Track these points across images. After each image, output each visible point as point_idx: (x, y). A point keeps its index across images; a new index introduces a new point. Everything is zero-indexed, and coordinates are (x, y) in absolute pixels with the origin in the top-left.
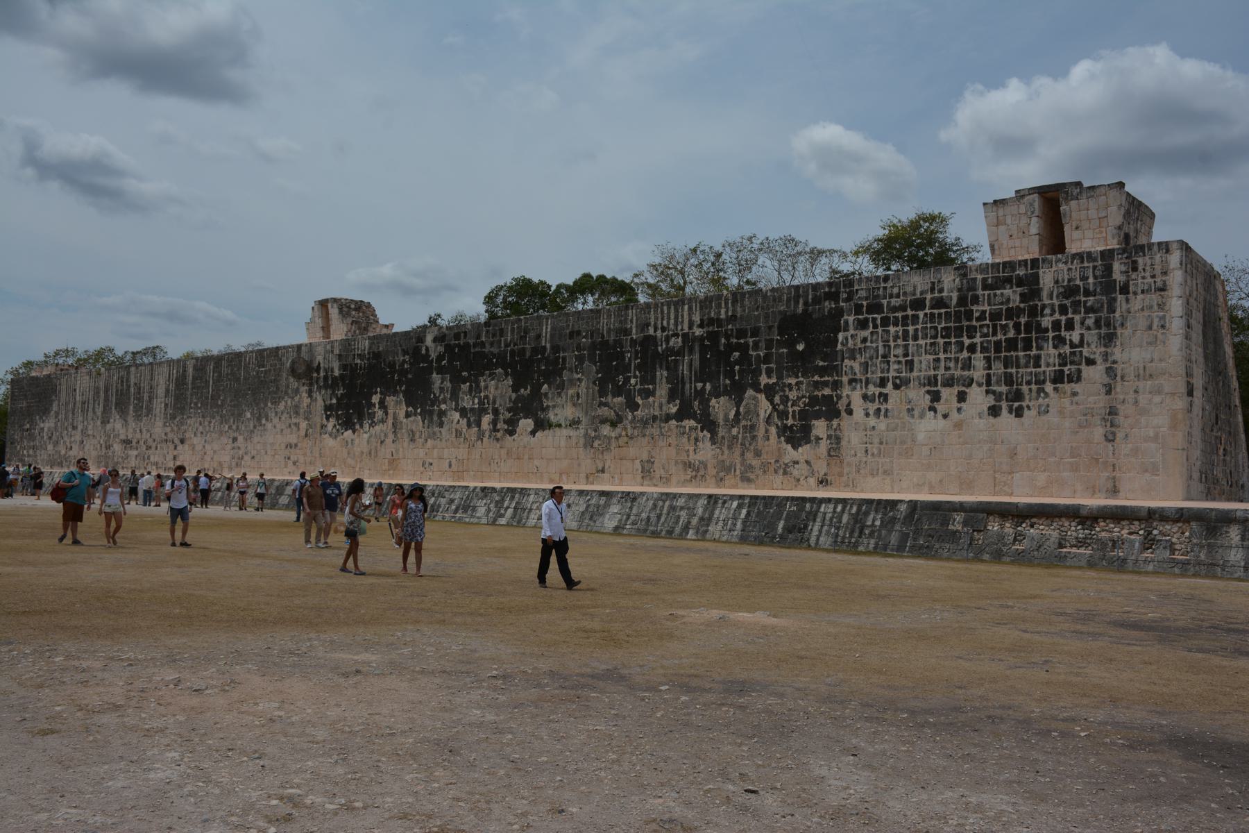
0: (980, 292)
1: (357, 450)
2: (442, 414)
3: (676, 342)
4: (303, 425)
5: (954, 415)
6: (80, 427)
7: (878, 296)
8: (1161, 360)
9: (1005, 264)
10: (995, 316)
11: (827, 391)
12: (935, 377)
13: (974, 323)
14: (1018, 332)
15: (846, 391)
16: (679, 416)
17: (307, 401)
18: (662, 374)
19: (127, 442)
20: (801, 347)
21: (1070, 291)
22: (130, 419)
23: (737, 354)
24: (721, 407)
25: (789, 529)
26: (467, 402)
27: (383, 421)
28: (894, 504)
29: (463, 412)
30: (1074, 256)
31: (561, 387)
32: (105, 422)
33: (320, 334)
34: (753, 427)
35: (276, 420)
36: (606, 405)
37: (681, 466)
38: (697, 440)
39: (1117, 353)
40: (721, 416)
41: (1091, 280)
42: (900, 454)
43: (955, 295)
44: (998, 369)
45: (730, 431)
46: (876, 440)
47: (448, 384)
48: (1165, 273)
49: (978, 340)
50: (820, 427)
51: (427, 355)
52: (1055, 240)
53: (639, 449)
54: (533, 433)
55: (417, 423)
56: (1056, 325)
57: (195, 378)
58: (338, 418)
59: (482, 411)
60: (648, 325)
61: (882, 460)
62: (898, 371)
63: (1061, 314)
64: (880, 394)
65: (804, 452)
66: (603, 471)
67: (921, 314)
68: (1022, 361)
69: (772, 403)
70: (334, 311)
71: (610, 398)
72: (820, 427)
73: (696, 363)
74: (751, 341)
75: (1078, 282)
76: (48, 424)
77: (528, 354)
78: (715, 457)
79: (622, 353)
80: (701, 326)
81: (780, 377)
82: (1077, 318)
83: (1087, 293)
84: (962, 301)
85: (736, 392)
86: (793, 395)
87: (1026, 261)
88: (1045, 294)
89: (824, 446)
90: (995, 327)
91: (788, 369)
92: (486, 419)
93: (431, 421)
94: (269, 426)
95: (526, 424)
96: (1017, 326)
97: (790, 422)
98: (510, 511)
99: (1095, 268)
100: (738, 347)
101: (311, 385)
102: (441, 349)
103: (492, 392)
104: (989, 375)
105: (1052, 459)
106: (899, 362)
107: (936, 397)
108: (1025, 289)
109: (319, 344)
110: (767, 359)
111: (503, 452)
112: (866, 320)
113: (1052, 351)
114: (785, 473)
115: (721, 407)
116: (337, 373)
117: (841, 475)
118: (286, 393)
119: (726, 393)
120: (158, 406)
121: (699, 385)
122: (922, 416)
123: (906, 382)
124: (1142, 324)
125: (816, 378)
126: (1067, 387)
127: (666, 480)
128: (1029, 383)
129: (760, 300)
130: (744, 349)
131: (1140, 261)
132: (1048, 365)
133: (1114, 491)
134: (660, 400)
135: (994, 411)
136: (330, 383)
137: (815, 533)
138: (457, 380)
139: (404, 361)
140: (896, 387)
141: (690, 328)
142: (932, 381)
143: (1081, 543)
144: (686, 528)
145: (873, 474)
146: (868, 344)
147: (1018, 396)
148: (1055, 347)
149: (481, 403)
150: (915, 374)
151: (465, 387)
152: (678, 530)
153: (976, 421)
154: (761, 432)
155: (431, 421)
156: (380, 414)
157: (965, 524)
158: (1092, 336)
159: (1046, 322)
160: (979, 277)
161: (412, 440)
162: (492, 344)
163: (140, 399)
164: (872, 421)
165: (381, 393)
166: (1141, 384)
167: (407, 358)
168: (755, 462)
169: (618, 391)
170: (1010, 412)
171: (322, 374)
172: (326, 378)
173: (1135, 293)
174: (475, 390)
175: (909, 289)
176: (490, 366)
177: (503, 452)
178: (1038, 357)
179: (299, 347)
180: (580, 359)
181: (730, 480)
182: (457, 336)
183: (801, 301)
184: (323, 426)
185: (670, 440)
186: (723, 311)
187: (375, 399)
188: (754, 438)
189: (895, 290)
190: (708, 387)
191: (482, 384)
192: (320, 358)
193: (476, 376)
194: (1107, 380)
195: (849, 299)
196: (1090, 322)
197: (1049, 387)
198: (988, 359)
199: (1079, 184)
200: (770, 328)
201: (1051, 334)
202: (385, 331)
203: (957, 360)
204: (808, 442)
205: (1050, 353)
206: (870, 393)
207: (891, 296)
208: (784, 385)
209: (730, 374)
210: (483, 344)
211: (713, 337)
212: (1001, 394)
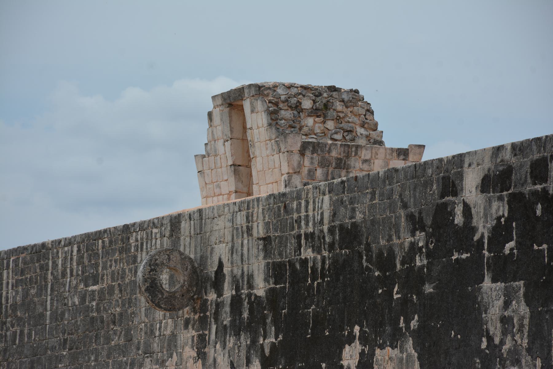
33: (229, 184)
47: (521, 309)
51: (469, 228)
70: (257, 119)
101: (203, 323)
109: (219, 212)
116: (261, 289)
136: (248, 317)
139: (414, 249)
165: (364, 340)
167: (420, 238)
171: (228, 293)
172: (236, 302)
179: (175, 221)
192: (221, 251)
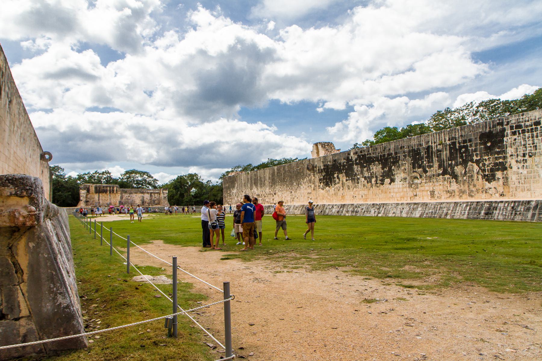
1: (331, 193)
2: (358, 179)
4: (313, 186)
7: (519, 122)
11: (501, 160)
15: (509, 159)
16: (444, 173)
17: (313, 178)
18: (435, 159)
20: (489, 144)
22: (259, 188)
23: (463, 149)
24: (459, 170)
25: (486, 214)
26: (366, 174)
27: (338, 183)
28: (529, 202)
31: (399, 167)
32: (251, 189)
34: (472, 176)
35: (304, 185)
36: (416, 172)
38: (450, 182)
45: (463, 178)
46: (523, 178)
50: (499, 174)
51: (352, 159)
53: (428, 187)
54: (390, 184)
55: (350, 183)
57: (277, 173)
58: (324, 183)
59: (372, 177)
60: (429, 142)
61: (525, 185)
62: (531, 150)
64: (523, 160)
65: (493, 184)
66: (416, 196)
69: (479, 166)
70: (320, 146)
71: (417, 169)
72: (499, 174)
73: (448, 155)
74: (469, 144)
76: (235, 191)
77: (386, 156)
78: (458, 188)
79: (420, 153)
80: (449, 140)
81: (481, 157)
85: (464, 163)
86: (487, 163)
89: (501, 181)
91: (484, 153)
92: (373, 180)
93: (355, 182)
94: (302, 187)
95: (387, 181)
97: (487, 173)
98: (383, 211)
100: (464, 147)
101: (314, 172)
102: (356, 157)
106: (531, 147)
110: (476, 150)
111: (380, 191)
112: (515, 132)
114: (486, 192)
115: (459, 170)
116: (322, 168)
117: (509, 192)
119: (461, 164)
120: (267, 183)
121: (450, 162)
125: (496, 156)
129: (471, 128)
130: (466, 147)
134: (435, 168)
136: (320, 171)
137: (497, 215)
138: (362, 167)
141: (445, 141)
144: (446, 214)
146: (517, 141)
149: (371, 174)
150: (538, 151)
151: (365, 169)
152: (443, 216)
155: (355, 182)
156: (337, 181)
161: (349, 189)
162: (373, 154)
163: (261, 181)
164: (521, 171)
168: (474, 189)
169: (419, 167)
172: (319, 170)
174: (369, 170)
175: (533, 118)
176: (373, 161)
180: (405, 156)
181: (464, 196)
182: (361, 152)
183: (488, 127)
184: (319, 186)
185: (440, 183)
186: (457, 134)
187: (335, 176)
188: (473, 180)
189: (527, 119)
190: (453, 162)
192: (316, 163)
193: (369, 165)
195: (508, 124)
200: (476, 138)
202: (338, 152)
204: (495, 180)
206: (519, 160)
207: (525, 121)
208: (483, 159)
209: (461, 157)
210: (370, 154)
211: (454, 144)
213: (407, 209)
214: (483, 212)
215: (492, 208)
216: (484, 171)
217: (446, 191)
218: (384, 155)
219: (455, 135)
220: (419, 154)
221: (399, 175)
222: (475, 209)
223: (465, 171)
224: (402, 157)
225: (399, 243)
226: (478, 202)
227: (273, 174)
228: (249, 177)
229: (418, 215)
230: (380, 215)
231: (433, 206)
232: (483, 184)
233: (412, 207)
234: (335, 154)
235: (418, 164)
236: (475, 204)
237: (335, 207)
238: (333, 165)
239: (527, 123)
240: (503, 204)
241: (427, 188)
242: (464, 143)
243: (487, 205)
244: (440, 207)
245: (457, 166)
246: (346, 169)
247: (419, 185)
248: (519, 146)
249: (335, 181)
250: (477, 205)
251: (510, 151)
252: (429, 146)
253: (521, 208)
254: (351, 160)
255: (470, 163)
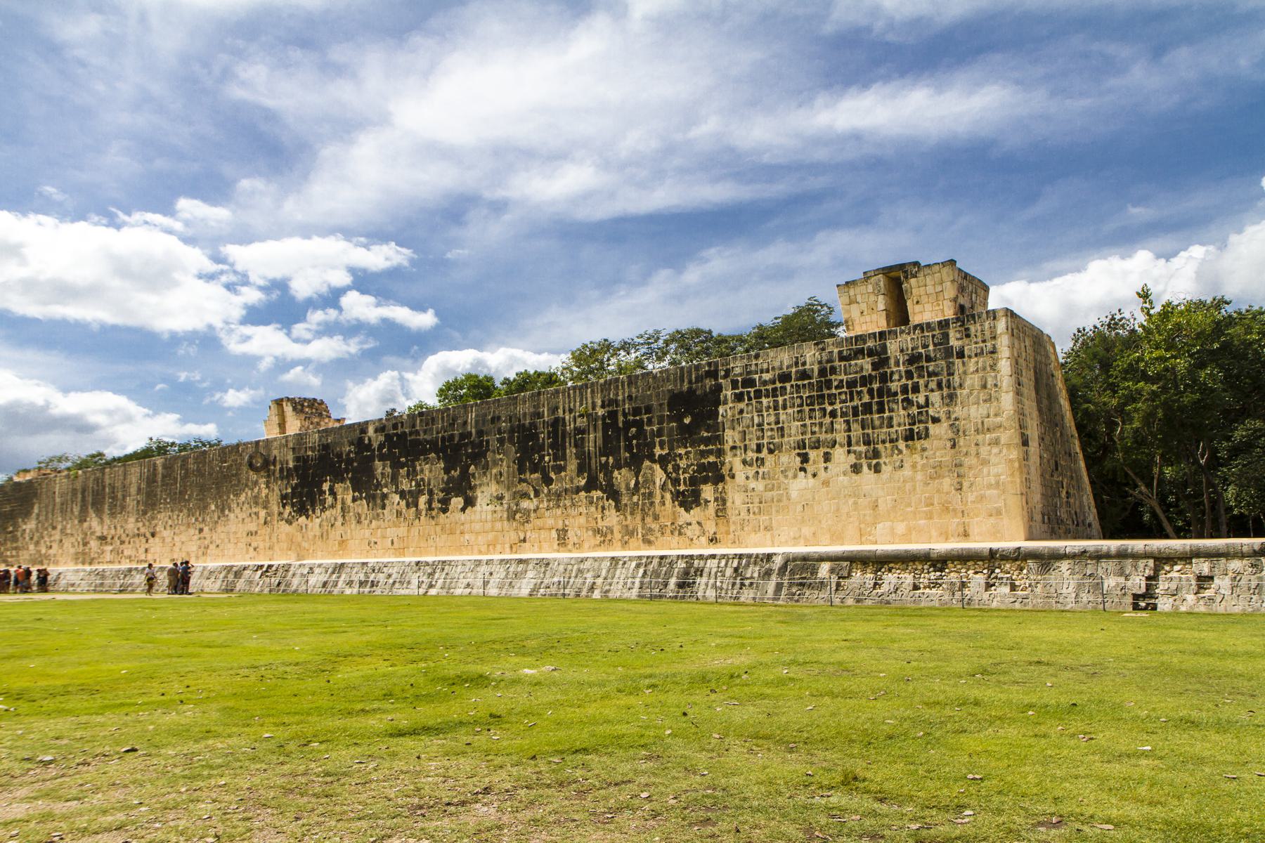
0: (837, 363)
1: (311, 534)
2: (385, 496)
3: (582, 423)
4: (263, 513)
5: (822, 474)
6: (59, 527)
7: (749, 373)
8: (996, 415)
9: (856, 337)
10: (852, 384)
11: (712, 459)
12: (803, 441)
13: (834, 391)
14: (872, 398)
15: (728, 458)
16: (588, 488)
17: (265, 492)
18: (571, 451)
19: (103, 538)
20: (687, 421)
21: (914, 359)
23: (634, 430)
24: (622, 478)
25: (681, 586)
26: (405, 485)
27: (333, 506)
28: (769, 557)
29: (403, 494)
30: (915, 327)
31: (486, 467)
32: (82, 521)
34: (651, 495)
35: (237, 511)
36: (525, 481)
37: (590, 533)
38: (603, 508)
39: (958, 411)
40: (623, 486)
41: (931, 348)
42: (778, 511)
43: (816, 368)
44: (857, 431)
45: (631, 499)
47: (388, 470)
48: (994, 338)
49: (837, 406)
50: (708, 491)
51: (370, 444)
52: (899, 313)
53: (552, 519)
54: (463, 510)
56: (905, 389)
57: (164, 477)
59: (420, 492)
60: (557, 408)
62: (772, 437)
63: (907, 379)
65: (696, 512)
66: (524, 540)
67: (788, 385)
68: (877, 423)
69: (666, 472)
70: (288, 409)
72: (708, 491)
73: (600, 442)
75: (921, 350)
76: (30, 525)
77: (457, 439)
78: (620, 523)
80: (603, 406)
81: (671, 449)
82: (922, 382)
83: (929, 359)
84: (822, 372)
85: (635, 463)
86: (683, 463)
87: (874, 334)
88: (892, 362)
90: (851, 393)
91: (678, 441)
92: (423, 499)
93: (375, 504)
94: (232, 516)
95: (457, 502)
96: (870, 392)
97: (682, 488)
98: (440, 581)
99: (933, 336)
101: (269, 476)
103: (427, 475)
104: (849, 437)
105: (909, 509)
106: (772, 430)
107: (805, 459)
108: (876, 359)
109: (275, 439)
110: (660, 433)
111: (438, 528)
112: (742, 393)
113: (902, 412)
114: (680, 534)
115: (622, 478)
116: (291, 465)
117: (728, 533)
118: (247, 485)
119: (628, 465)
120: (130, 503)
121: (604, 459)
122: (795, 476)
123: (779, 447)
124: (977, 384)
125: (702, 447)
126: (918, 444)
127: (578, 546)
128: (884, 442)
130: (639, 424)
131: (972, 329)
132: (899, 425)
133: (966, 535)
134: (570, 475)
135: (856, 469)
136: (286, 474)
138: (396, 465)
139: (350, 451)
140: (771, 451)
141: (594, 408)
142: (801, 445)
143: (934, 584)
144: (592, 589)
145: (756, 530)
147: (876, 454)
148: (904, 409)
149: (418, 485)
150: (786, 439)
151: (403, 471)
152: (584, 593)
153: (841, 478)
154: (657, 500)
155: (375, 504)
156: (330, 500)
157: (832, 571)
158: (935, 397)
159: (894, 386)
160: (836, 350)
161: (359, 522)
162: (425, 432)
163: (114, 498)
164: (752, 484)
166: (980, 437)
168: (655, 526)
170: (869, 467)
171: (278, 467)
172: (281, 470)
173: (970, 357)
174: (412, 474)
175: (777, 364)
176: (425, 452)
177: (438, 528)
178: (891, 418)
179: (257, 443)
180: (501, 441)
182: (395, 427)
184: (280, 514)
185: (581, 509)
187: (326, 487)
188: (652, 504)
189: (765, 366)
190: (611, 460)
191: (418, 468)
192: (275, 452)
193: (413, 461)
194: (951, 435)
196: (933, 385)
197: (901, 444)
198: (848, 422)
199: (916, 264)
201: (900, 397)
202: (337, 425)
203: (821, 425)
204: (698, 504)
205: (900, 414)
209: (629, 448)
210: (417, 433)
211: (613, 415)
212: (860, 453)
213: (500, 572)
214: (673, 581)
215: (692, 570)
216: (676, 482)
217: (594, 531)
218: (452, 436)
219: (617, 395)
220: (536, 436)
221: (486, 492)
222: (656, 574)
223: (637, 483)
224: (494, 444)
225: (429, 698)
226: (662, 558)
227: (151, 480)
228: (78, 485)
229: (525, 592)
230: (433, 592)
231: (561, 568)
232: (674, 513)
233: (511, 569)
234: (326, 431)
235: (532, 462)
236: (655, 561)
237: (317, 571)
238: (321, 458)
239: (766, 377)
240: (716, 561)
241: (550, 522)
242: (634, 415)
243: (682, 565)
244: (580, 571)
245: (619, 469)
246: (355, 471)
247: (532, 515)
248: (748, 427)
249: (323, 502)
250: (660, 564)
251: (731, 437)
252: (557, 420)
253: (753, 571)
254: (369, 447)
255: (647, 463)
